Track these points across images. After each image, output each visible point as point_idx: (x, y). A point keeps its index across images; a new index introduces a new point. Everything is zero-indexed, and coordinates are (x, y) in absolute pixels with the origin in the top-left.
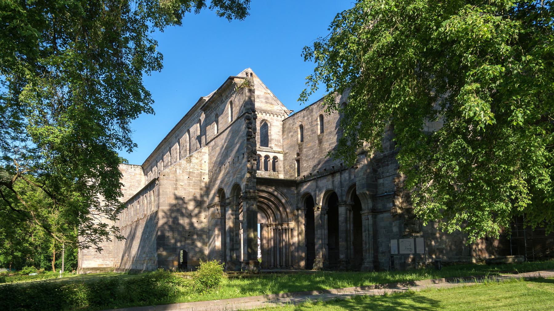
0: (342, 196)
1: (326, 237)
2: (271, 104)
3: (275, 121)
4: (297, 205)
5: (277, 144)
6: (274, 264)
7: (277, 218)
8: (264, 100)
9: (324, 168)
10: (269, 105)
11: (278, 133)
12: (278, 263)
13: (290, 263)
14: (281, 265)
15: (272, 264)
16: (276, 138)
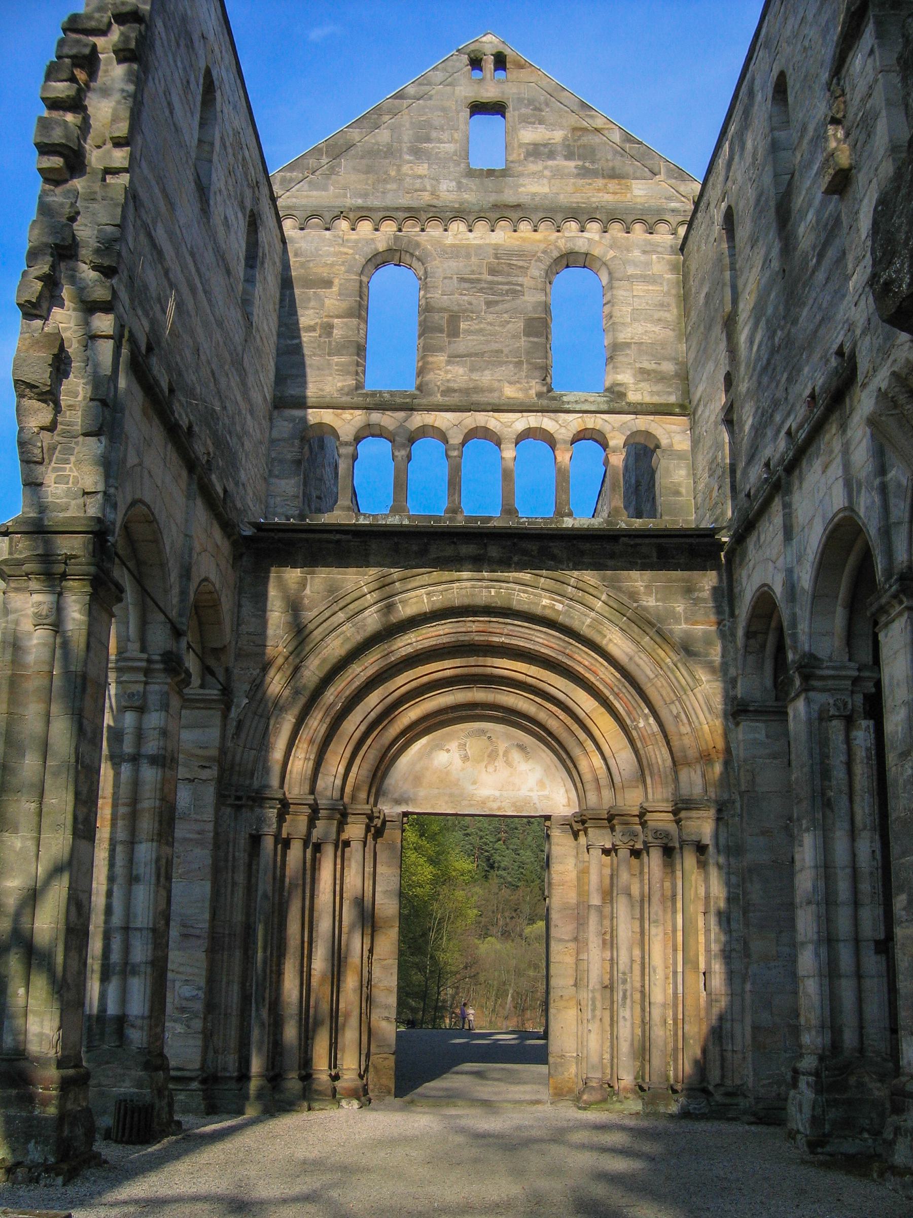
0: (886, 532)
2: (614, 175)
3: (636, 254)
5: (646, 365)
8: (572, 164)
9: (807, 392)
10: (600, 182)
11: (657, 315)
16: (646, 339)
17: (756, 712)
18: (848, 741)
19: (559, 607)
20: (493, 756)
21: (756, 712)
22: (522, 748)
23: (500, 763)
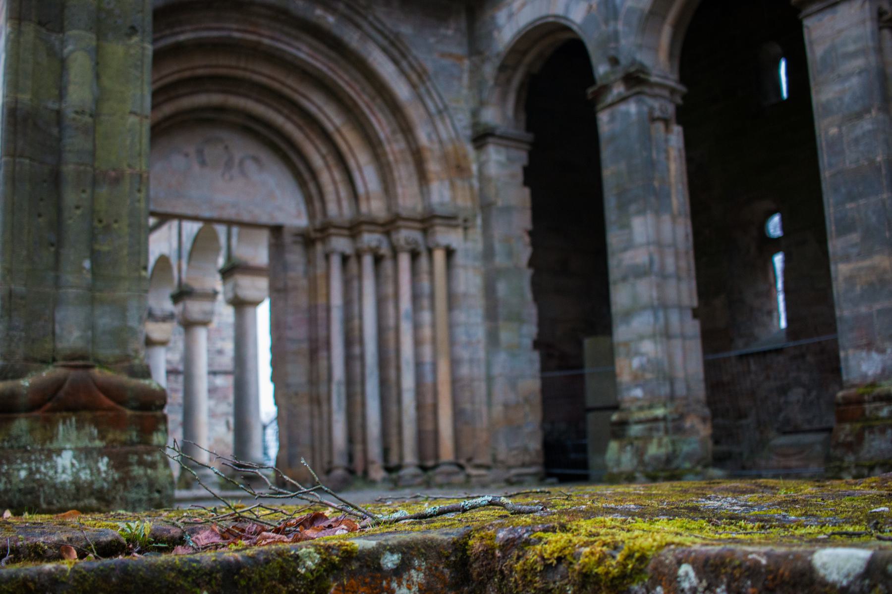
1: (683, 264)
4: (475, 113)
6: (351, 457)
7: (361, 189)
12: (375, 450)
13: (447, 451)
14: (394, 460)
15: (340, 461)
17: (501, 137)
18: (667, 141)
19: (331, 19)
20: (228, 165)
21: (501, 137)
22: (256, 160)
23: (235, 171)
